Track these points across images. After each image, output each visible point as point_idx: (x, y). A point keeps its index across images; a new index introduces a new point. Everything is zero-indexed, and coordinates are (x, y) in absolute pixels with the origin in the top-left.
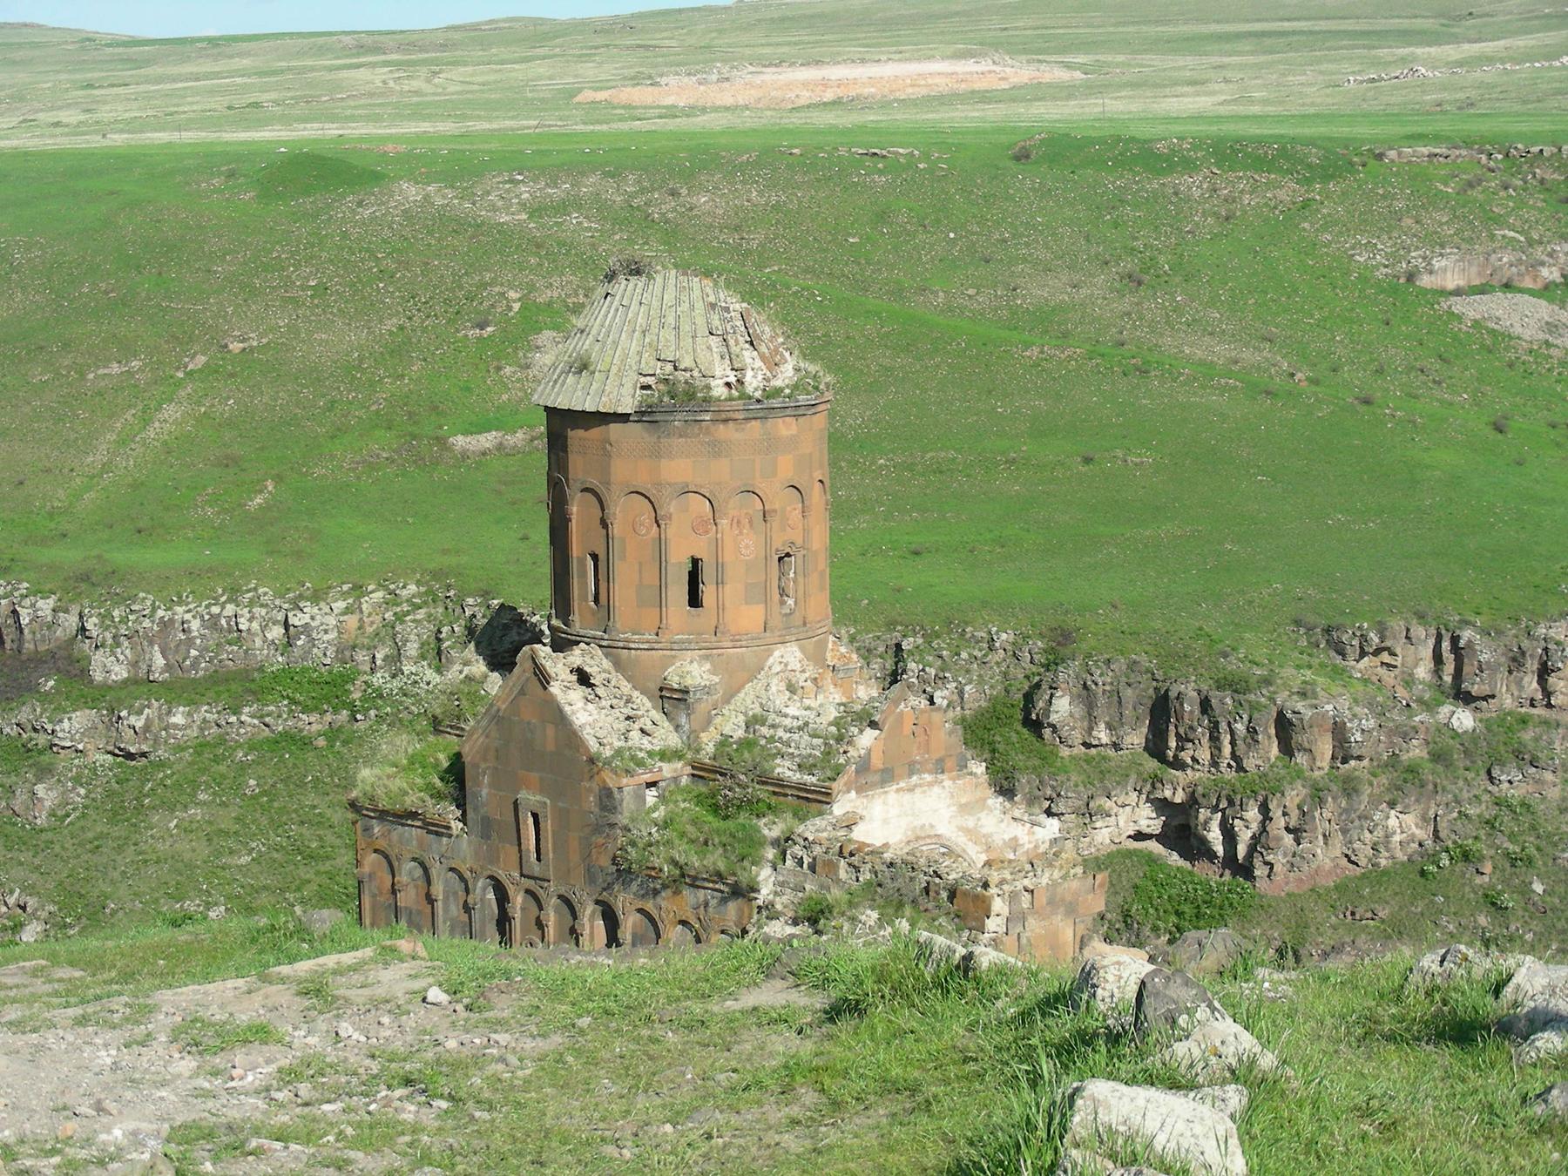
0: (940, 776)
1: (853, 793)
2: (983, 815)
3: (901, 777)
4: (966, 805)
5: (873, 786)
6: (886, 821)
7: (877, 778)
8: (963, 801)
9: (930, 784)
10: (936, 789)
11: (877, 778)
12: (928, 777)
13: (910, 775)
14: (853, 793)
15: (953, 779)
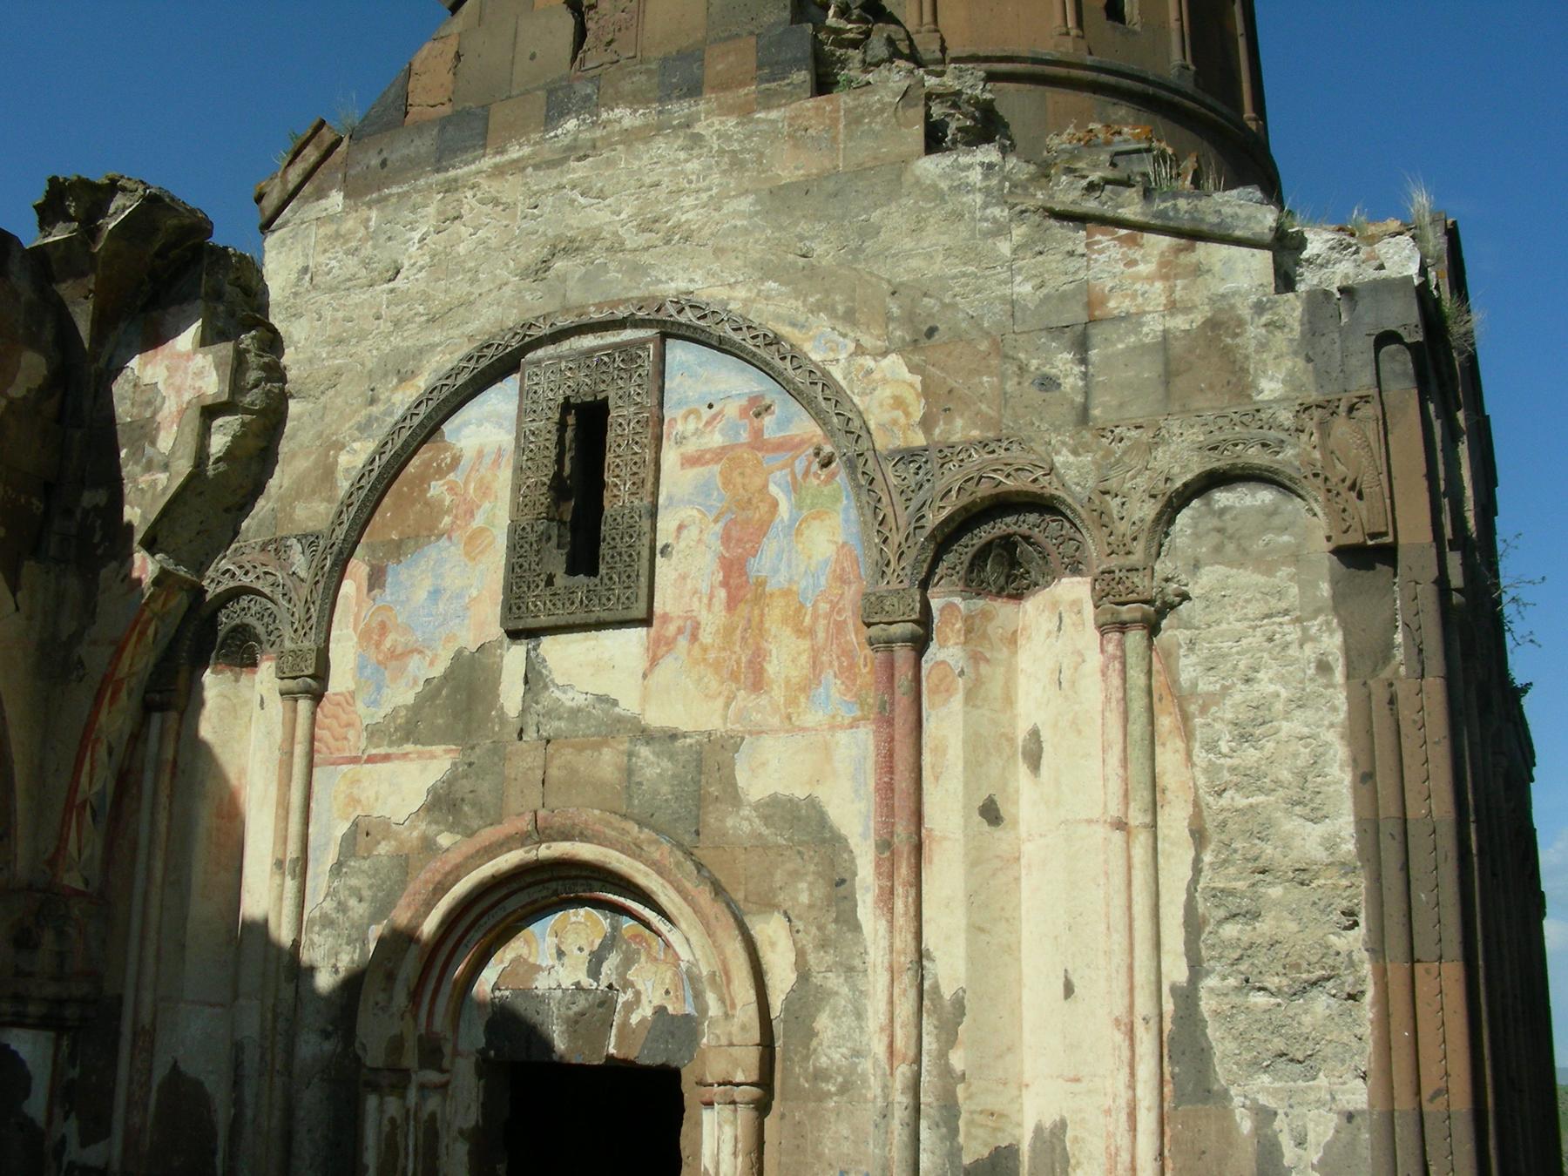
0: (679, 109)
1: (336, 200)
2: (892, 219)
3: (515, 131)
4: (804, 189)
5: (412, 167)
6: (441, 264)
7: (424, 145)
8: (788, 168)
9: (630, 137)
10: (660, 146)
11: (424, 145)
12: (624, 117)
13: (553, 115)
14: (336, 200)
15: (744, 111)
